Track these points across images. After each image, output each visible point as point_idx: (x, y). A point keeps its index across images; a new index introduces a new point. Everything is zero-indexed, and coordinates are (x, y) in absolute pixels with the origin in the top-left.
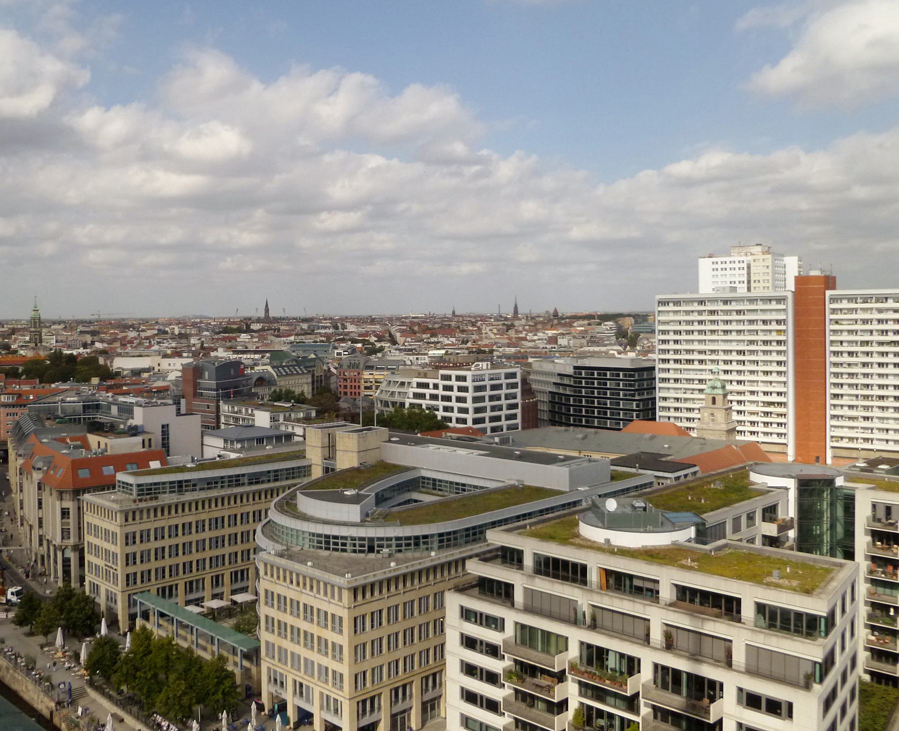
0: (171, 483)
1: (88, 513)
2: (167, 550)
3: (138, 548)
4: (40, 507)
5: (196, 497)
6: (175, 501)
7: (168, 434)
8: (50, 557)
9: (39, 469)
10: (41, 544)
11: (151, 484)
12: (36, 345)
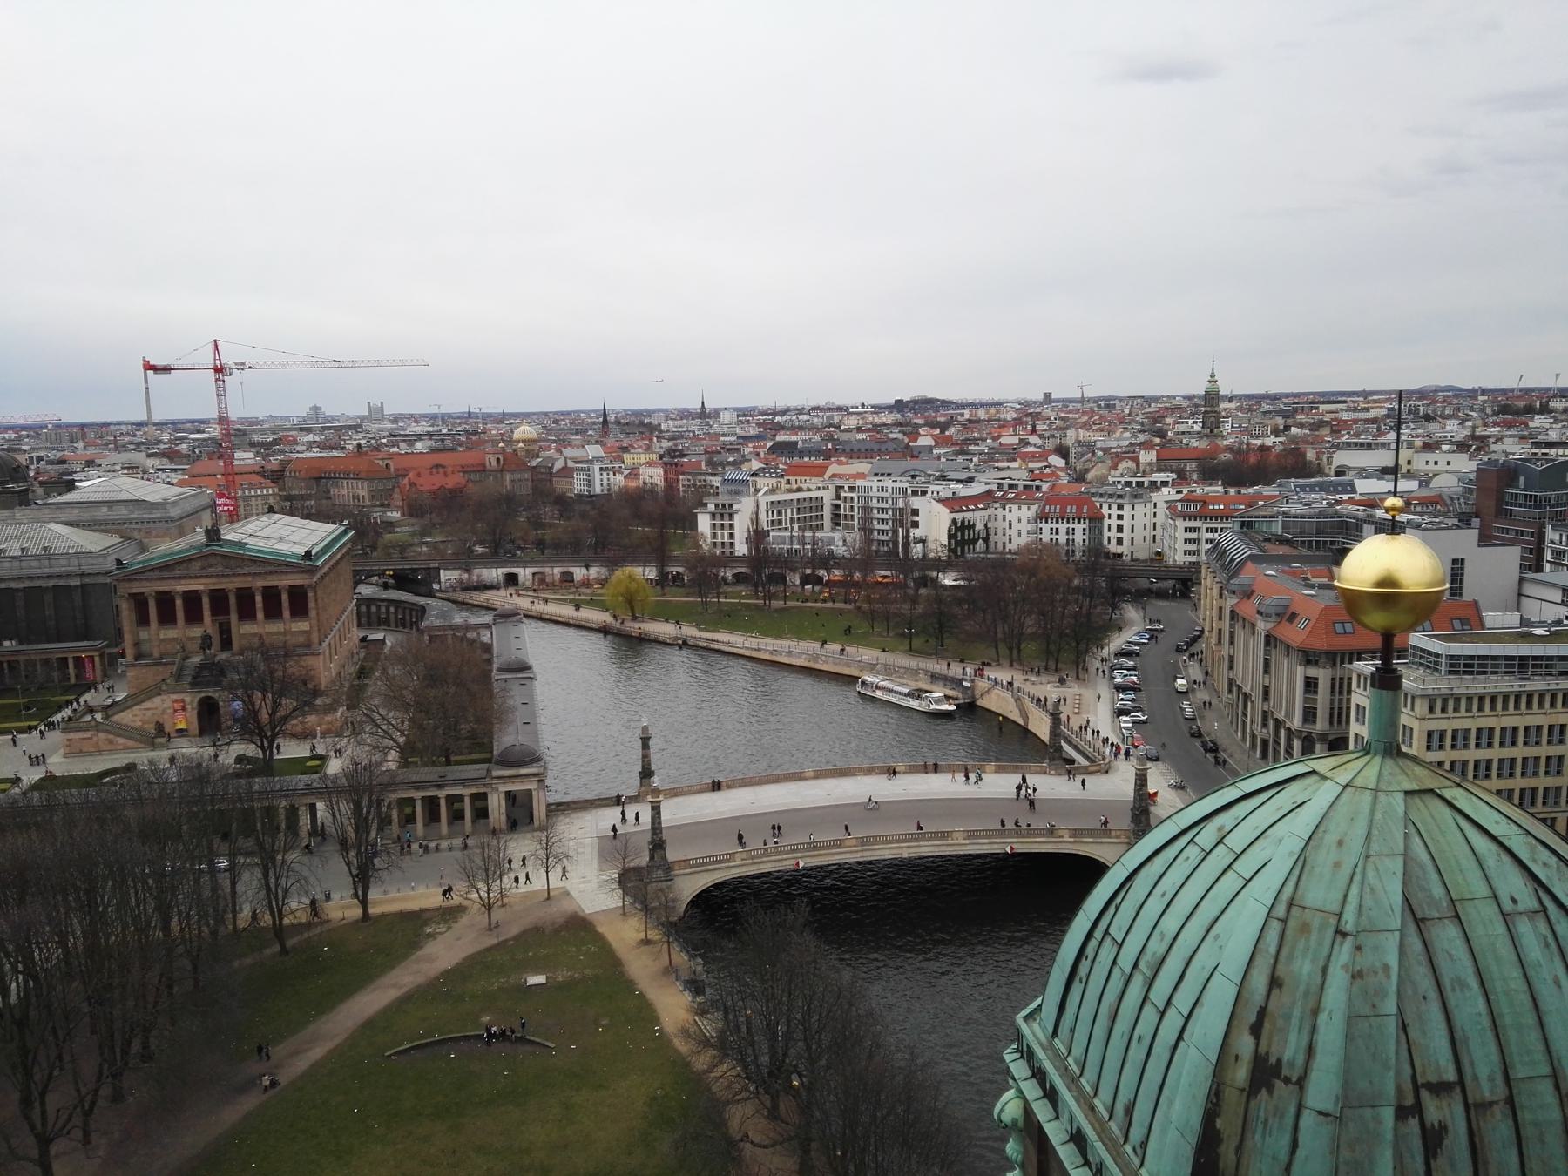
0: (1508, 658)
1: (1361, 691)
2: (1495, 765)
3: (1447, 756)
4: (1267, 671)
5: (1553, 687)
6: (1516, 689)
7: (1462, 575)
8: (1279, 744)
9: (1268, 615)
10: (1265, 725)
11: (1472, 657)
12: (1212, 431)
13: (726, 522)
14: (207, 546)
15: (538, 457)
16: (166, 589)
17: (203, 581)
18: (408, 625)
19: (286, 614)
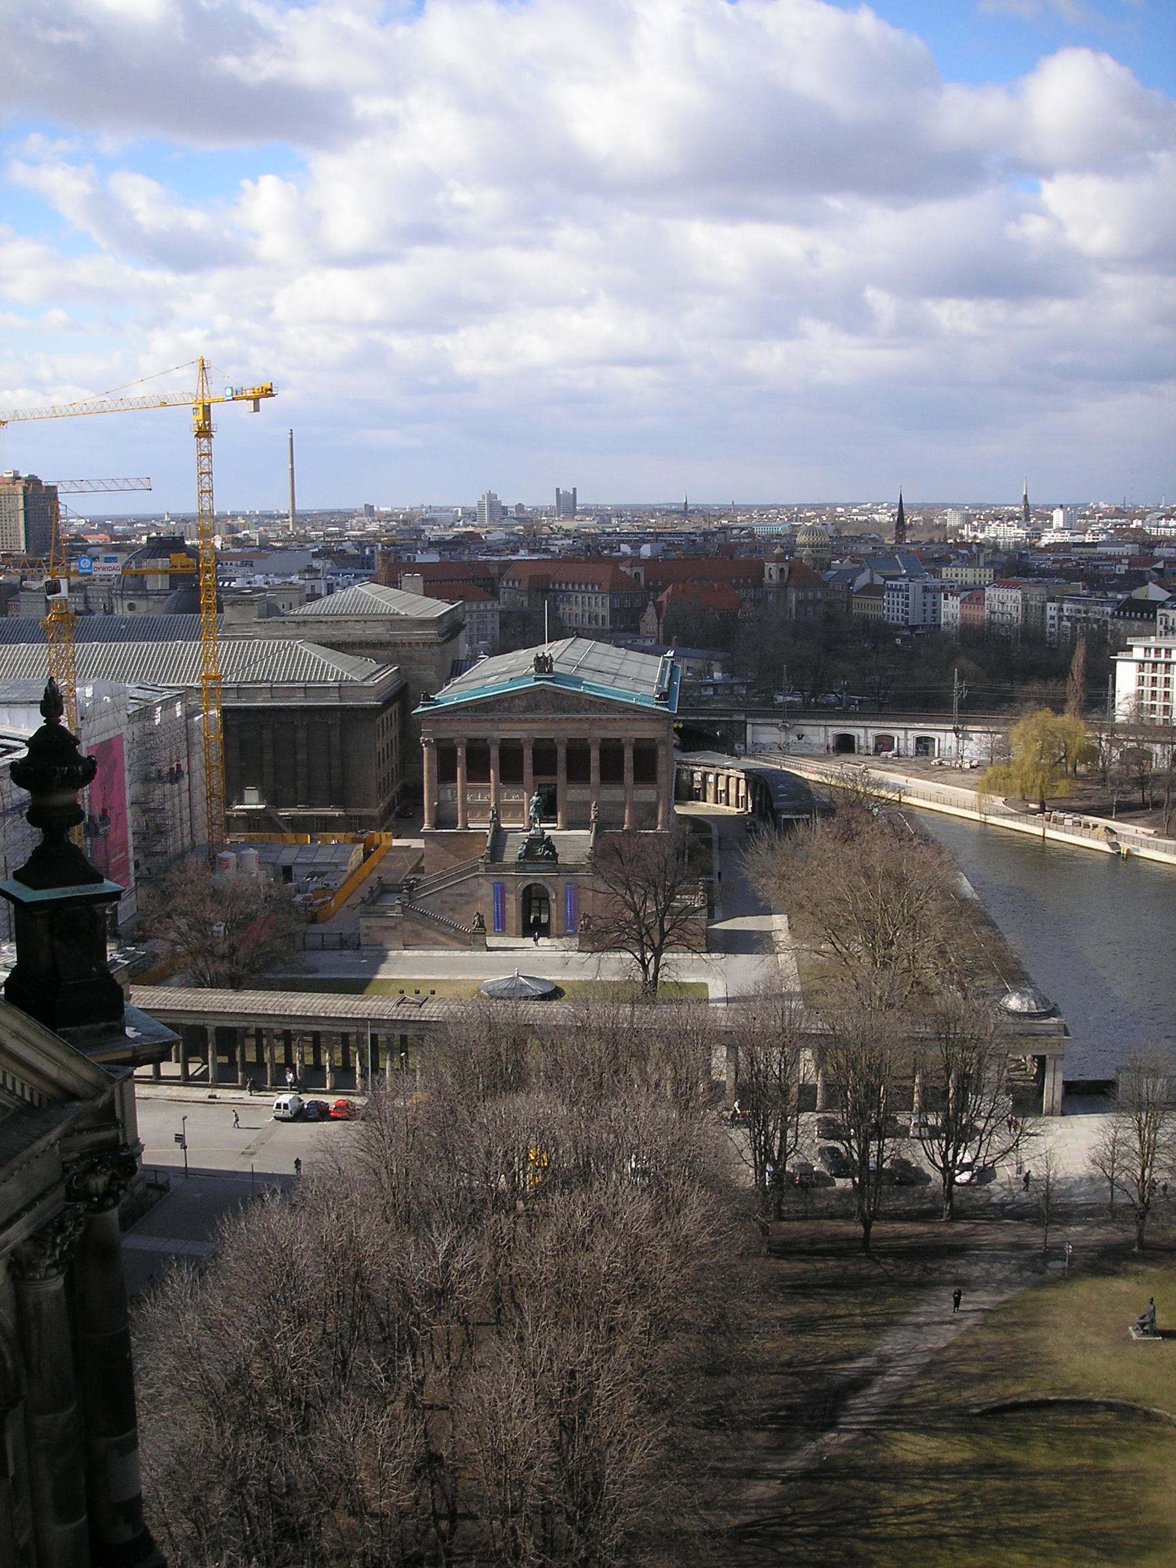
13: (1160, 675)
14: (536, 679)
15: (829, 568)
16: (481, 734)
17: (526, 726)
18: (732, 800)
19: (629, 777)
